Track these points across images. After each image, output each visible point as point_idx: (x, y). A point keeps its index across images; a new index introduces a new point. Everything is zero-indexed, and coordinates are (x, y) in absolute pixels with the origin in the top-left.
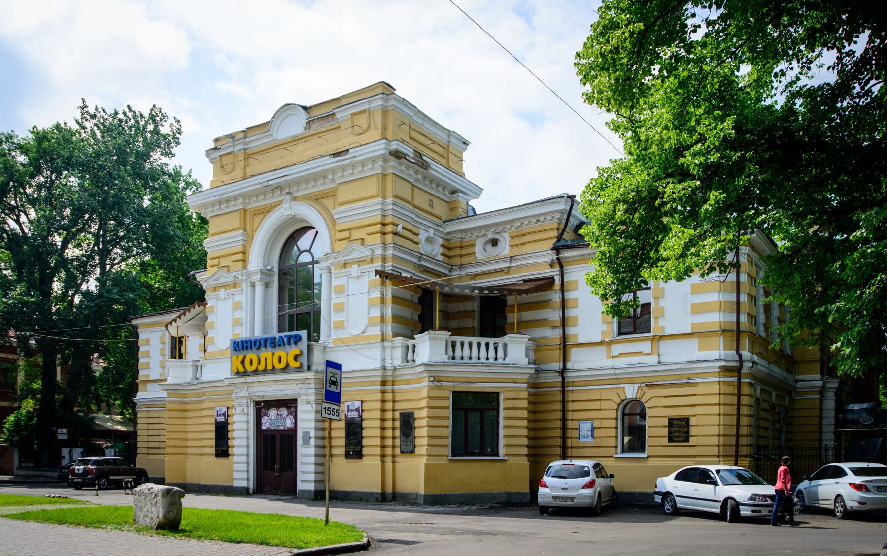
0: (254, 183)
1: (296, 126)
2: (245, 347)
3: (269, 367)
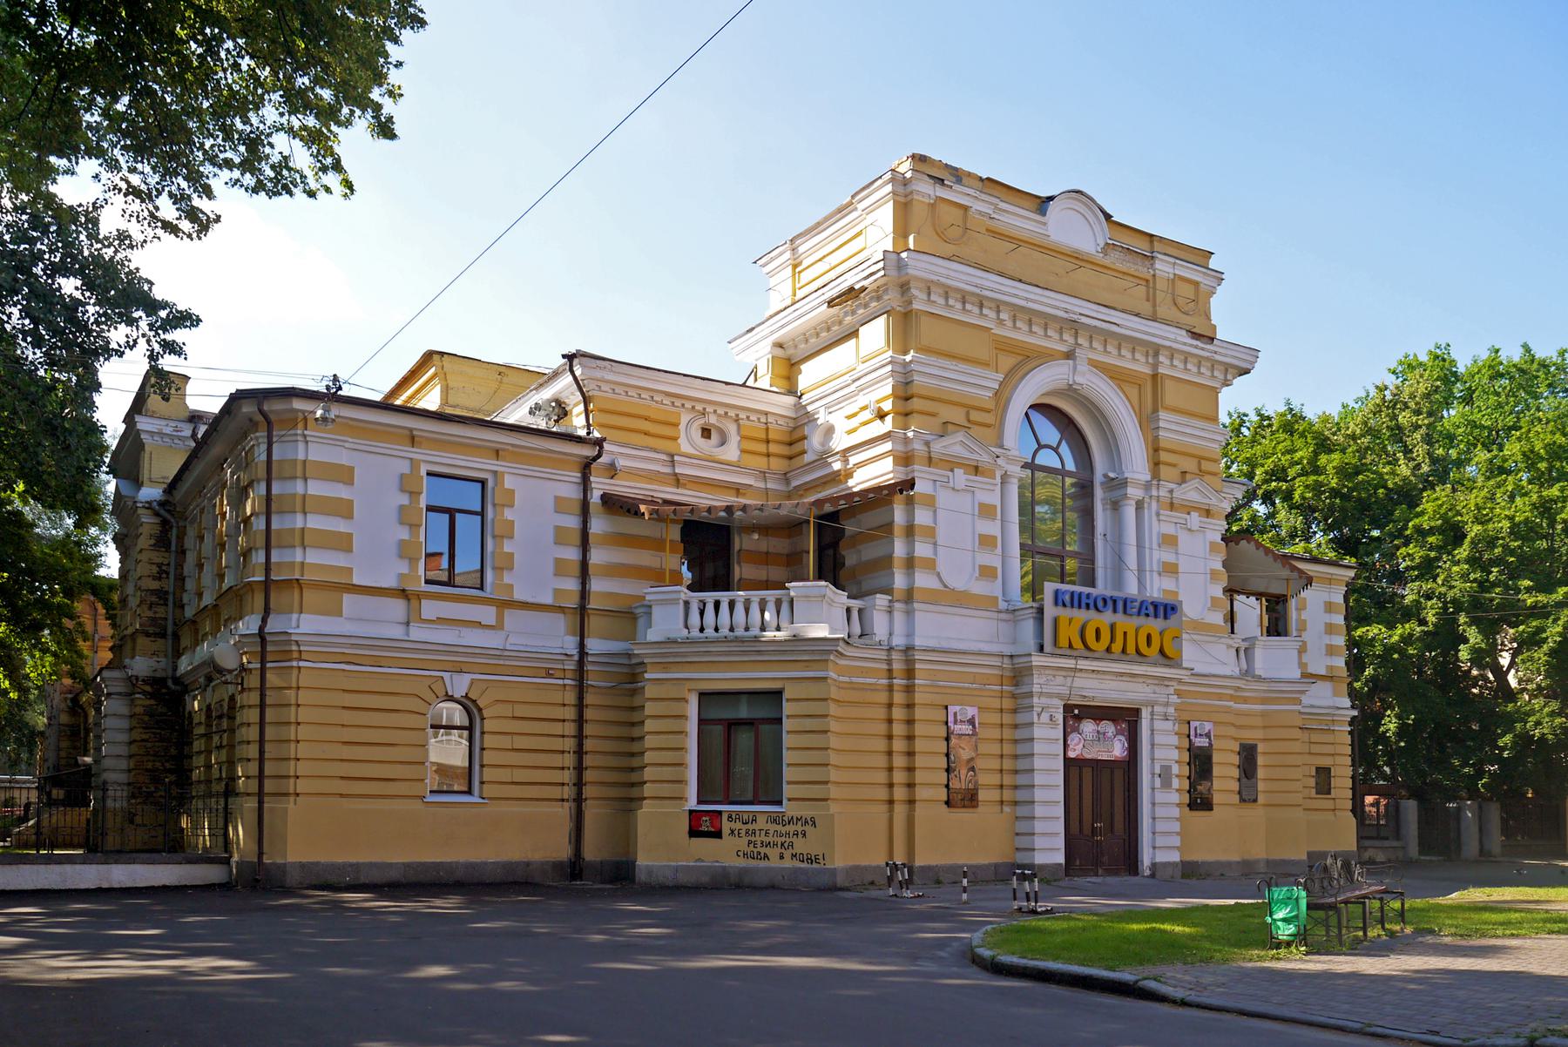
0: (1057, 304)
1: (1085, 238)
2: (1083, 605)
3: (1117, 647)
